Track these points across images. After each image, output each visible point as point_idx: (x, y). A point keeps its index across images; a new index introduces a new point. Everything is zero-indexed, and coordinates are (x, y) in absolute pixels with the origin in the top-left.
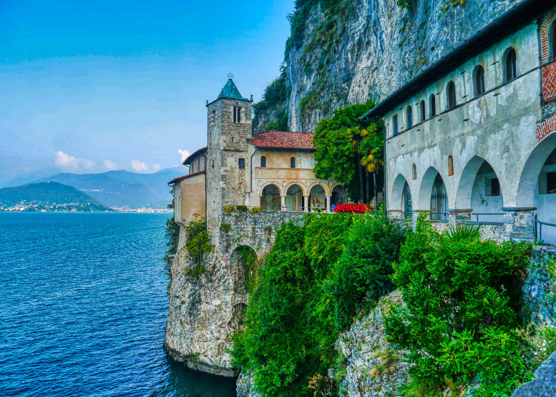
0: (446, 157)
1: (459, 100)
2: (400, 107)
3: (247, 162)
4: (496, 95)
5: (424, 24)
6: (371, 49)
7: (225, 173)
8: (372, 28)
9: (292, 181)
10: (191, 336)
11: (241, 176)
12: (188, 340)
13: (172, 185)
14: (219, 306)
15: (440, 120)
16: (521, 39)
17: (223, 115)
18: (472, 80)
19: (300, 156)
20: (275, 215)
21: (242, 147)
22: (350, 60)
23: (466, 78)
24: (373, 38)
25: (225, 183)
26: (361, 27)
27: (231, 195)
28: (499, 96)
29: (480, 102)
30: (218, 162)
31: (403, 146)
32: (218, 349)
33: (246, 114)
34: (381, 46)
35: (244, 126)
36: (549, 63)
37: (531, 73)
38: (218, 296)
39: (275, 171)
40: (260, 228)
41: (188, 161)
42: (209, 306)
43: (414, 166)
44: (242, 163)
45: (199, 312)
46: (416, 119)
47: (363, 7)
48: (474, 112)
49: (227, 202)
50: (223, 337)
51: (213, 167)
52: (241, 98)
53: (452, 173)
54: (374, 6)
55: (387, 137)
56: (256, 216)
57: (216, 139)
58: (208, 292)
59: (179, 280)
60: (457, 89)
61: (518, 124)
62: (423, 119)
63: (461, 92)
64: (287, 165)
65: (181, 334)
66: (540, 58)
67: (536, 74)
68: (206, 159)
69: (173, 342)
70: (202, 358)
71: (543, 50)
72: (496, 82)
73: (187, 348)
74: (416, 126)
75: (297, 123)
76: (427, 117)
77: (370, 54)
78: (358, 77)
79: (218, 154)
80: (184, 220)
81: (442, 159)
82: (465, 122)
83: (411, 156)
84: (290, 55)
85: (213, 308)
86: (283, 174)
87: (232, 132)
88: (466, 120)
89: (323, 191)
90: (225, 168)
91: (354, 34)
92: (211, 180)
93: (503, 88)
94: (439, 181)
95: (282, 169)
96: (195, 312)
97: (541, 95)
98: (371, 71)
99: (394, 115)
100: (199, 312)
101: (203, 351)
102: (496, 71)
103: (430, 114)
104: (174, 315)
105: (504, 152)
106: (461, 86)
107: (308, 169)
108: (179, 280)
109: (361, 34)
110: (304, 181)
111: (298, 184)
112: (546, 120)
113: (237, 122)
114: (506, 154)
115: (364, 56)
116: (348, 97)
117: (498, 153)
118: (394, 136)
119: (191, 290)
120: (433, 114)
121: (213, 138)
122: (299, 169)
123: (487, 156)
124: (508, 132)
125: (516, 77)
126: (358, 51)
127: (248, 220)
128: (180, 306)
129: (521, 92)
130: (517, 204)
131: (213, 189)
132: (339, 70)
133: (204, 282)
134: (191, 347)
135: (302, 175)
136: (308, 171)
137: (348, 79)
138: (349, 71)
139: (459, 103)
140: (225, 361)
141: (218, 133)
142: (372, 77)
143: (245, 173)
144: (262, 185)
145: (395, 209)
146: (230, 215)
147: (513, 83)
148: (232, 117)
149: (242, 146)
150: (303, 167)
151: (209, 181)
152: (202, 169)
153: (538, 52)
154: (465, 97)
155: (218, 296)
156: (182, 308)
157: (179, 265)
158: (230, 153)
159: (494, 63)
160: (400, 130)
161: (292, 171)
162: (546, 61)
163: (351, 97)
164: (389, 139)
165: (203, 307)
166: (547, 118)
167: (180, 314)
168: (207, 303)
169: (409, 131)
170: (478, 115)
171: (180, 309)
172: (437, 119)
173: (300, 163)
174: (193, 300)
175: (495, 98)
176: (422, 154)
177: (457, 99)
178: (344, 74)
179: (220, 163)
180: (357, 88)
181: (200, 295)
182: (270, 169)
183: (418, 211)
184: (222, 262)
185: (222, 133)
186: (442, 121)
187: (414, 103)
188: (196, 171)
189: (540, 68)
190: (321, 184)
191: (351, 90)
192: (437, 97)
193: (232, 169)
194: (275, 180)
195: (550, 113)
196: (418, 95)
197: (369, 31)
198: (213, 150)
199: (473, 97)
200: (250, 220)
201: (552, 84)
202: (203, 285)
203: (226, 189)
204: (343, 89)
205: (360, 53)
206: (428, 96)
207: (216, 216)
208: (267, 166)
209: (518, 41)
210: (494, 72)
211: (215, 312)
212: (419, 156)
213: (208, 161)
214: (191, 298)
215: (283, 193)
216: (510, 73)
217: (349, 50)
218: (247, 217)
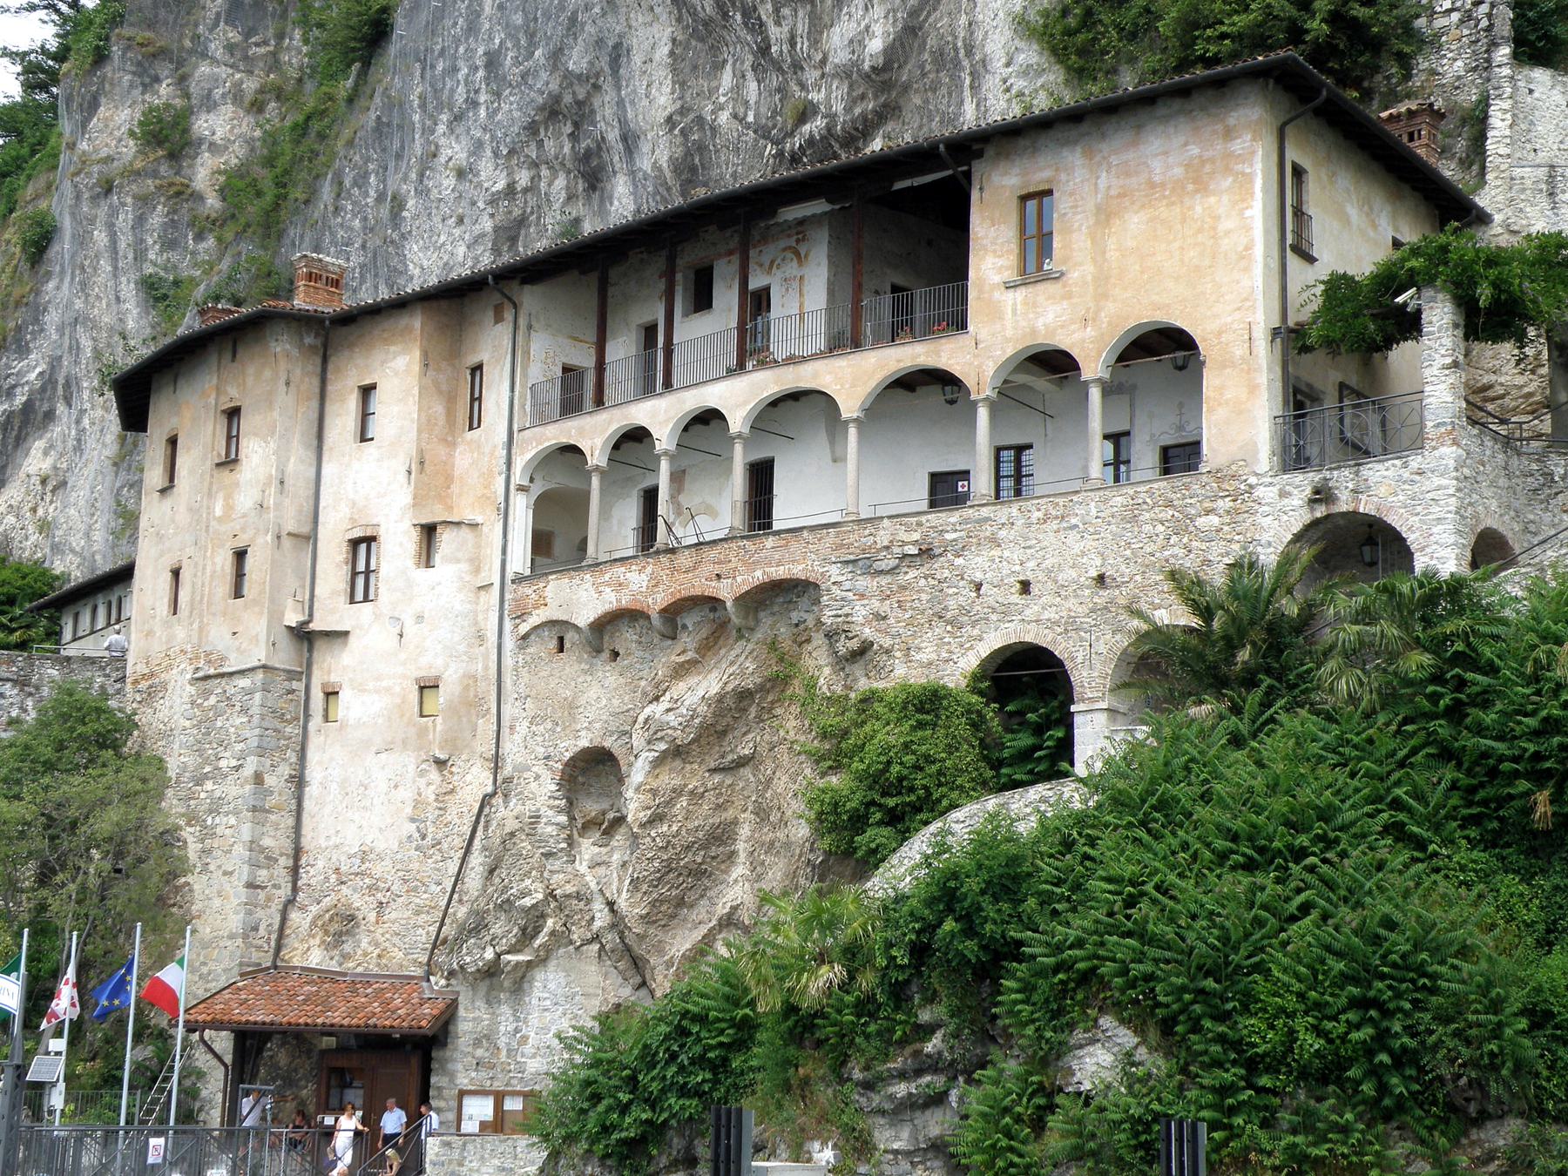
6: (56, 430)
8: (60, 387)
24: (61, 408)
26: (32, 376)
46: (101, 622)
47: (42, 330)
54: (70, 348)
77: (52, 446)
91: (14, 387)
98: (49, 487)
109: (31, 392)
115: (38, 445)
118: (74, 640)
142: (51, 502)
160: (80, 634)
197: (55, 389)
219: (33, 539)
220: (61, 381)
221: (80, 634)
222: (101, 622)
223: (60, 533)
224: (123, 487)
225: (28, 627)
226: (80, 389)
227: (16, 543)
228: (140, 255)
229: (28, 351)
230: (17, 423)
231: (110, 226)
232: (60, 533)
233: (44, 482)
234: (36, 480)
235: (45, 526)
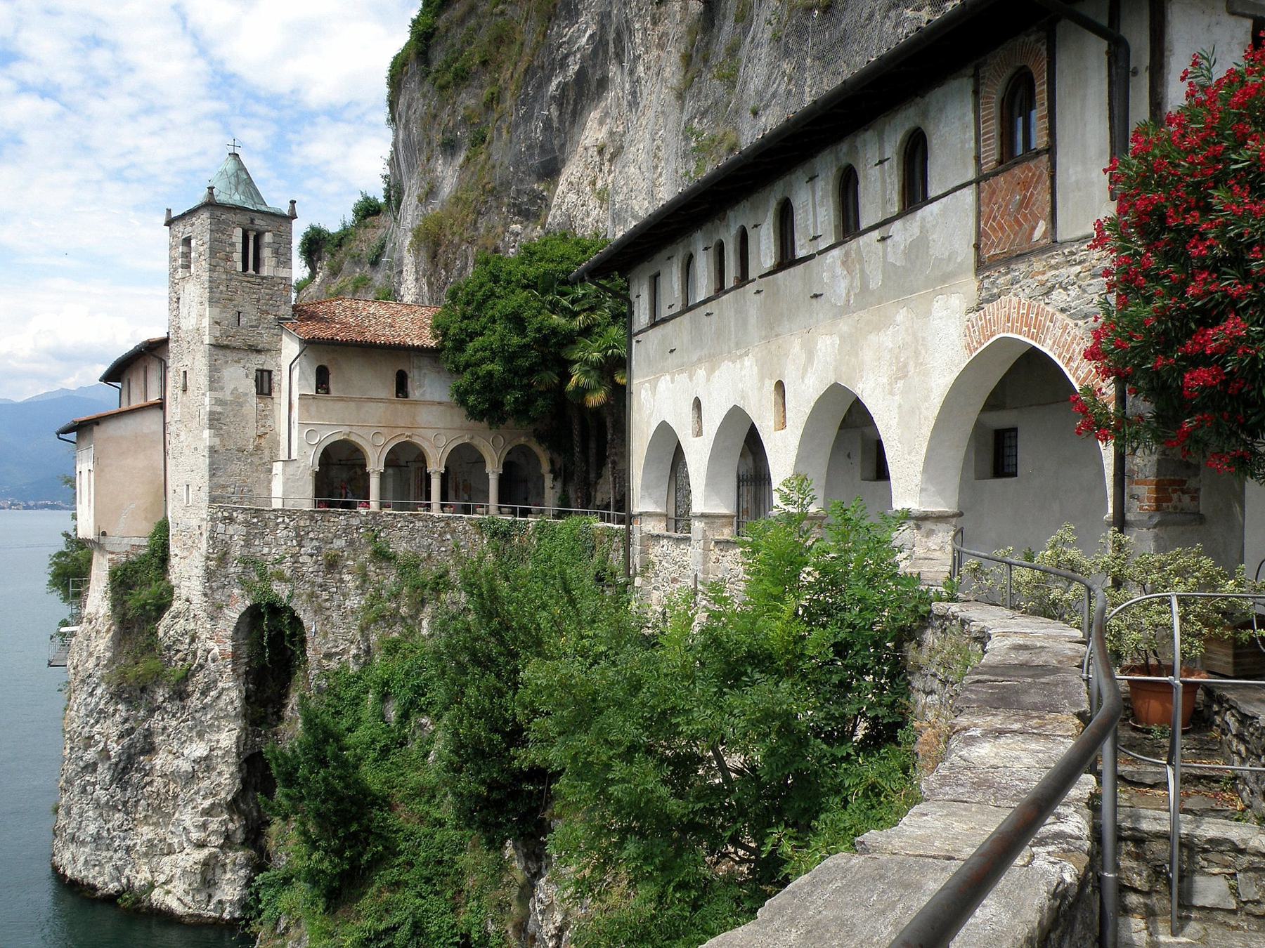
0: (770, 385)
1: (802, 246)
2: (665, 253)
3: (281, 379)
4: (883, 239)
5: (733, 51)
7: (219, 409)
8: (611, 45)
9: (399, 431)
10: (129, 842)
11: (264, 416)
12: (119, 854)
13: (72, 436)
14: (206, 758)
15: (758, 292)
16: (941, 110)
17: (213, 252)
18: (831, 199)
19: (420, 368)
21: (266, 338)
22: (555, 125)
23: (819, 194)
25: (216, 436)
27: (235, 467)
28: (889, 241)
29: (847, 254)
30: (199, 377)
31: (672, 351)
32: (202, 873)
33: (276, 252)
34: (634, 93)
35: (271, 282)
36: (996, 174)
37: (958, 193)
38: (201, 735)
39: (352, 404)
40: (312, 556)
41: (119, 372)
42: (176, 762)
43: (697, 404)
44: (264, 383)
45: (147, 779)
46: (703, 285)
48: (834, 277)
49: (224, 487)
50: (217, 840)
51: (185, 391)
52: (263, 208)
53: (782, 424)
55: (636, 329)
56: (302, 523)
57: (194, 314)
58: (174, 723)
59: (91, 694)
60: (799, 218)
61: (928, 313)
62: (721, 289)
63: (806, 226)
64: (389, 391)
65: (97, 838)
66: (978, 158)
67: (968, 195)
68: (165, 368)
69: (74, 860)
70: (157, 896)
71: (985, 140)
72: (884, 208)
73: (114, 873)
74: (704, 302)
75: (417, 280)
76: (730, 282)
77: (607, 114)
78: (572, 171)
79: (199, 356)
80: (104, 534)
81: (761, 388)
82: (814, 301)
83: (691, 378)
84: (402, 100)
85: (186, 766)
86: (377, 413)
87: (238, 298)
88: (816, 296)
89: (481, 461)
90: (219, 395)
92: (179, 425)
93: (898, 224)
94: (753, 443)
95: (370, 400)
96: (136, 777)
97: (977, 247)
98: (607, 156)
99: (652, 273)
100: (147, 779)
101: (162, 878)
102: (884, 181)
103: (736, 278)
104: (76, 790)
105: (897, 379)
106: (806, 211)
107: (439, 403)
108: (91, 694)
110: (430, 434)
111: (416, 440)
112: (986, 306)
113: (251, 271)
114: (900, 384)
116: (550, 220)
117: (885, 380)
118: (654, 325)
119: (126, 721)
120: (743, 279)
121: (183, 310)
122: (416, 402)
123: (860, 385)
124: (907, 330)
125: (927, 201)
126: (576, 104)
127: (281, 533)
128: (95, 764)
129: (934, 236)
130: (921, 504)
131: (186, 451)
132: (529, 148)
133: (161, 699)
134: (127, 872)
135: (426, 416)
136: (442, 408)
137: (550, 171)
138: (553, 150)
139: (800, 253)
140: (220, 902)
141: (198, 299)
142: (610, 172)
143: (272, 411)
144: (320, 442)
145: (651, 508)
146: (231, 520)
147: (920, 213)
148: (237, 256)
149: (265, 339)
150: (428, 397)
151: (171, 429)
152: (154, 398)
153: (972, 144)
154: (815, 238)
155: (201, 735)
156: (100, 769)
157: (91, 655)
158: (231, 356)
159: (881, 162)
160: (664, 312)
161: (399, 406)
162: (986, 168)
163: (554, 217)
164: (641, 332)
165: (159, 761)
166: (988, 301)
167: (94, 784)
168: (170, 752)
169: (688, 315)
170: (842, 286)
171: (95, 770)
172: (750, 288)
173: (420, 386)
174: (130, 746)
175: (880, 245)
176: (717, 373)
177: (798, 244)
178: (536, 161)
179: (204, 381)
180: (572, 197)
181: (149, 734)
182: (340, 399)
183: (703, 516)
184: (211, 644)
185: (210, 300)
186: (763, 294)
187: (700, 246)
188: (136, 402)
189: (977, 182)
190: (475, 442)
191: (556, 201)
192: (751, 234)
193: (238, 401)
194: (354, 429)
195: (995, 291)
196: (709, 225)
198: (185, 345)
199: (832, 241)
200: (285, 532)
201: (999, 223)
202: (159, 708)
203: (222, 450)
204: (536, 197)
205: (583, 108)
206: (734, 230)
207: (195, 523)
208: (333, 393)
209: (932, 114)
210: (879, 184)
211: (191, 777)
212: (708, 380)
213: (170, 375)
214: (126, 741)
215: (375, 465)
216: (914, 194)
217: (553, 97)
218: (278, 524)
219: (594, 214)
220: (612, 36)
221: (664, 312)
222: (703, 285)
223: (621, 197)
224: (692, 118)
225: (592, 309)
226: (631, 32)
227: (578, 221)
229: (578, 14)
230: (572, 95)
232: (621, 197)
233: (601, 151)
234: (593, 151)
235: (604, 197)
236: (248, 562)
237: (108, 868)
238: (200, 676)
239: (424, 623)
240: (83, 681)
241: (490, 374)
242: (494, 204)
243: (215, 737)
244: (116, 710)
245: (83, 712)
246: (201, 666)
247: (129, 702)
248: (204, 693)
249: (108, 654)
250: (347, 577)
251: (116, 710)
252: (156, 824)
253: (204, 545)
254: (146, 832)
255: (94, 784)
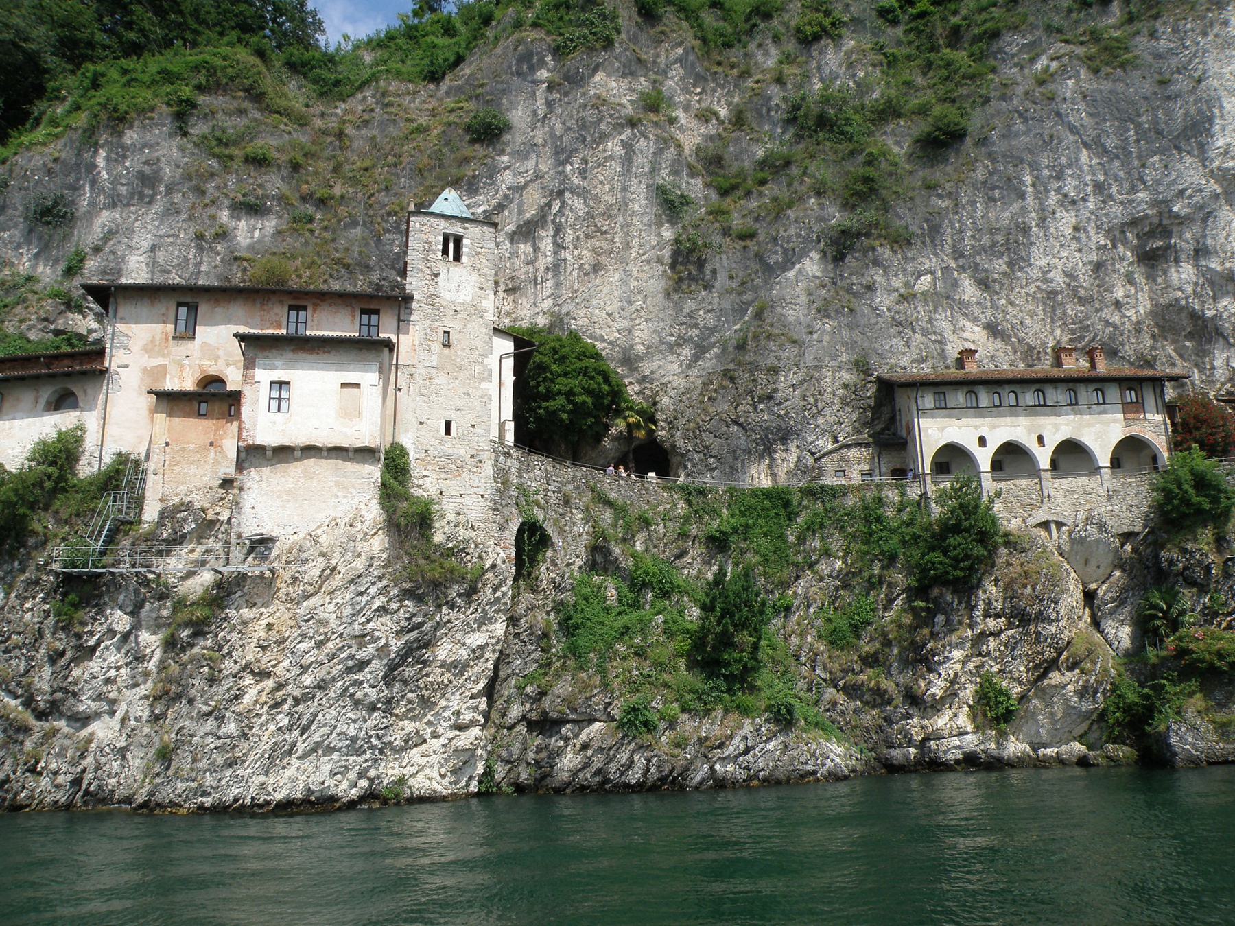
20: (579, 474)
85: (463, 654)
157: (359, 555)
167: (362, 682)
228: (653, 171)
231: (628, 146)
236: (521, 489)
237: (352, 775)
238: (489, 575)
239: (638, 544)
240: (352, 581)
241: (584, 403)
242: (347, 275)
243: (491, 627)
244: (401, 607)
245: (348, 611)
246: (493, 566)
247: (420, 599)
248: (495, 590)
249: (384, 555)
250: (574, 511)
251: (401, 607)
252: (413, 719)
253: (488, 469)
254: (409, 726)
255: (362, 682)
